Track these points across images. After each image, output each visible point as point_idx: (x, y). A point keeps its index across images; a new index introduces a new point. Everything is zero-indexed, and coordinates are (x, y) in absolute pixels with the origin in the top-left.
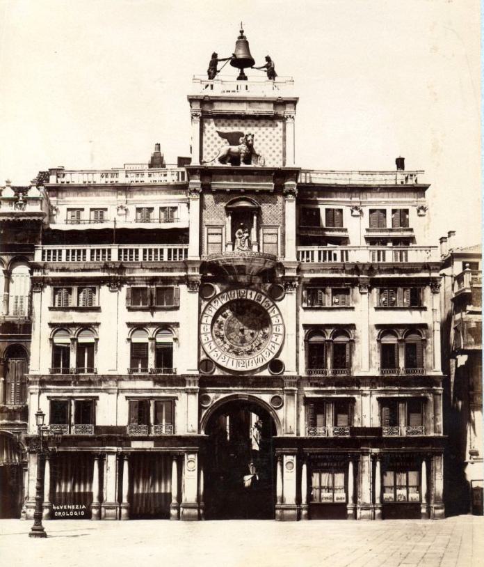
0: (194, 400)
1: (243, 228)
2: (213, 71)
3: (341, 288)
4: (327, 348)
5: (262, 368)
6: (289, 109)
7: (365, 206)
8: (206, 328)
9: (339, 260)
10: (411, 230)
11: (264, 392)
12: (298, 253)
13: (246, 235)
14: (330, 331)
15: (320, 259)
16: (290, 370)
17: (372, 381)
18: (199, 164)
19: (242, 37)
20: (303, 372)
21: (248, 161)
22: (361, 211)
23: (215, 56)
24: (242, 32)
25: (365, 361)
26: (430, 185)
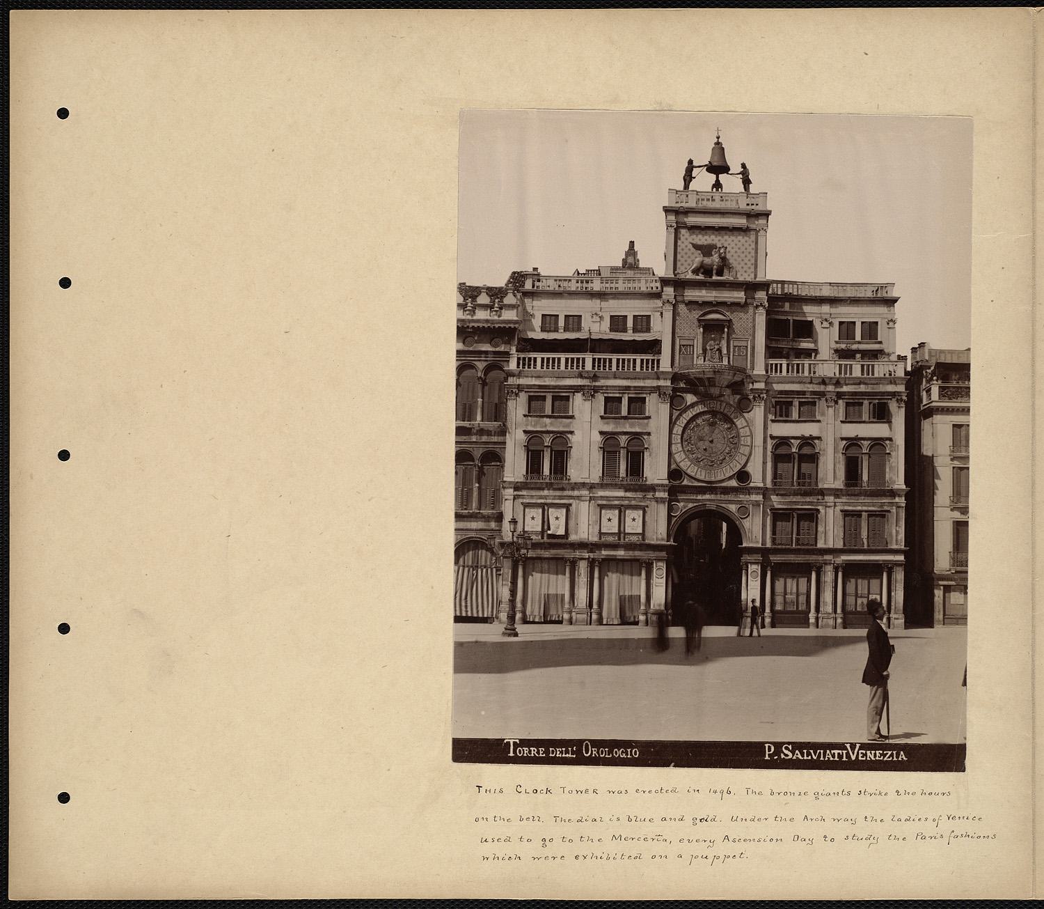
0: (663, 510)
1: (714, 340)
2: (688, 177)
3: (809, 406)
4: (795, 458)
5: (730, 478)
6: (762, 221)
7: (835, 318)
8: (677, 439)
9: (806, 373)
10: (881, 343)
11: (731, 502)
12: (767, 365)
13: (717, 347)
14: (796, 443)
15: (788, 372)
16: (756, 481)
17: (836, 493)
18: (673, 276)
19: (718, 143)
20: (769, 485)
21: (720, 273)
22: (831, 324)
23: (691, 162)
24: (718, 138)
25: (831, 472)
26: (899, 298)
